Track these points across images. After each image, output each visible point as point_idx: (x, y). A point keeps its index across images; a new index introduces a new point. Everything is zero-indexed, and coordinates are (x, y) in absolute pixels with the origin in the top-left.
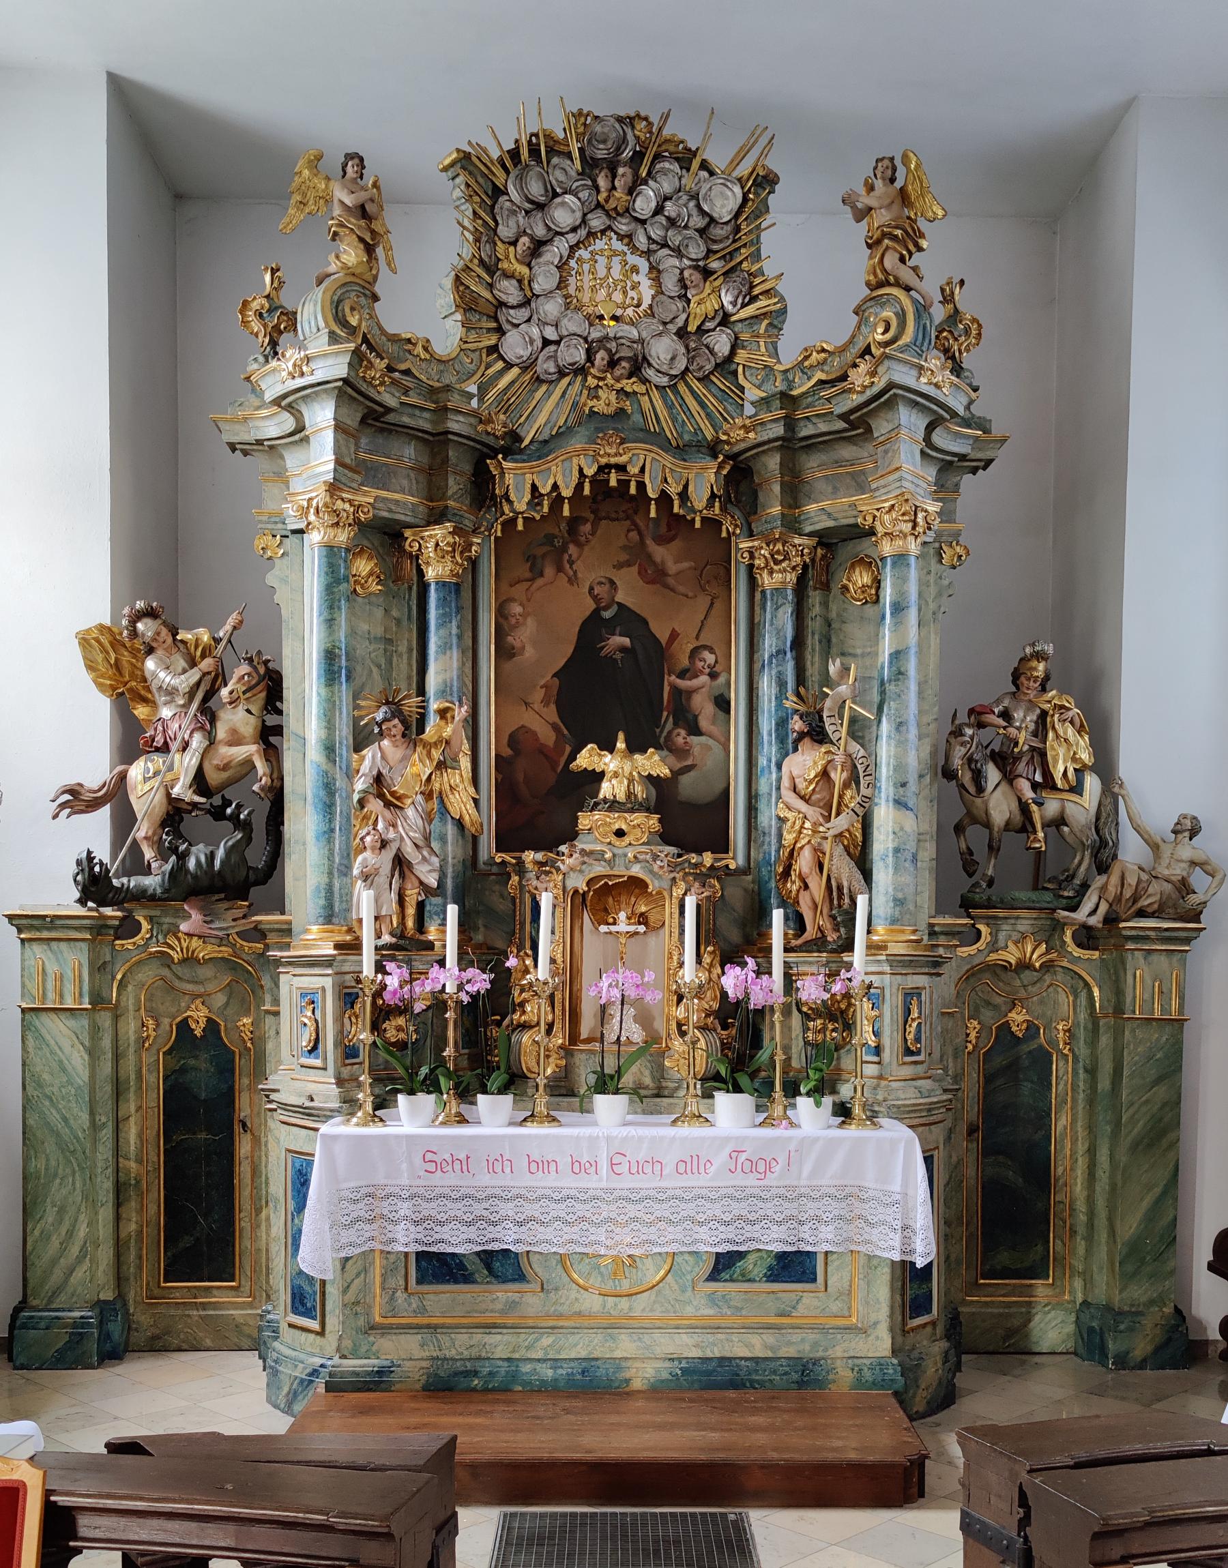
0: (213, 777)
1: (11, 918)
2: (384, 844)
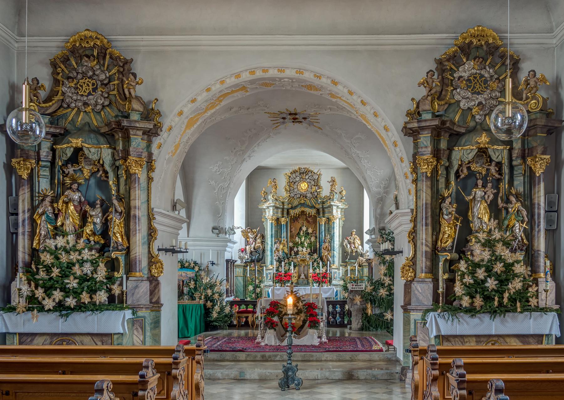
0: (256, 248)
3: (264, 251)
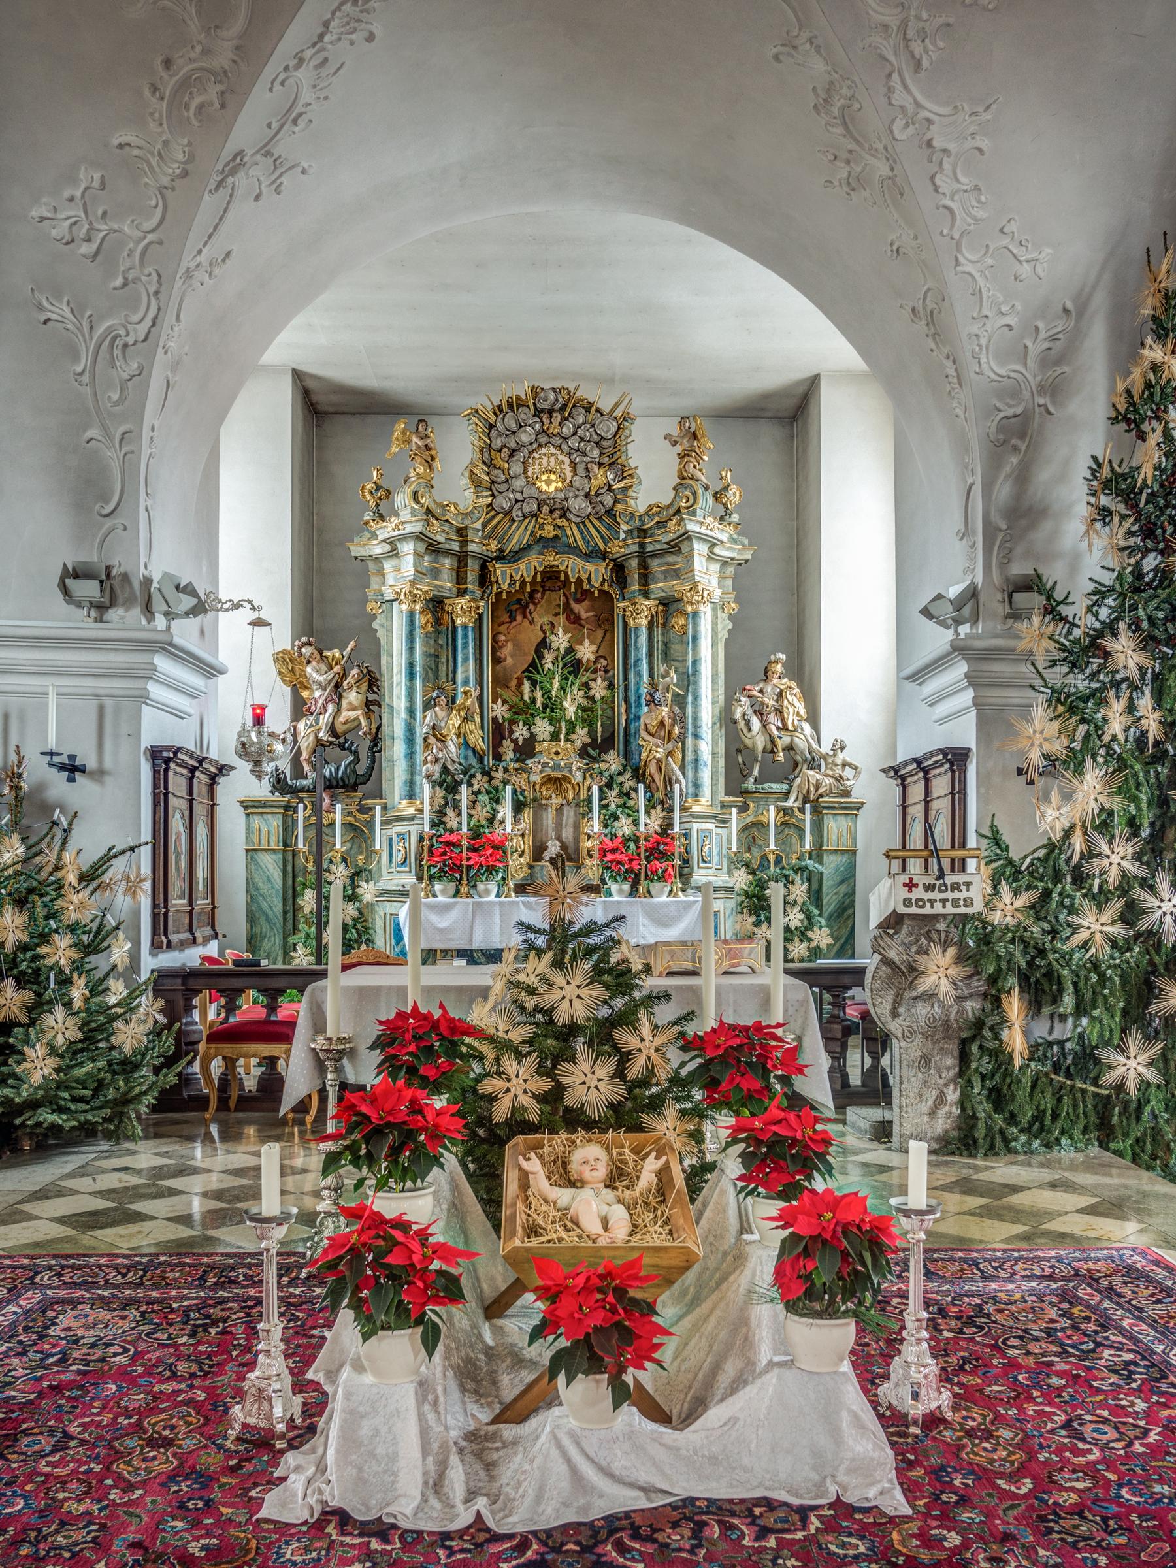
0: (340, 728)
1: (241, 802)
2: (437, 760)
3: (376, 741)
